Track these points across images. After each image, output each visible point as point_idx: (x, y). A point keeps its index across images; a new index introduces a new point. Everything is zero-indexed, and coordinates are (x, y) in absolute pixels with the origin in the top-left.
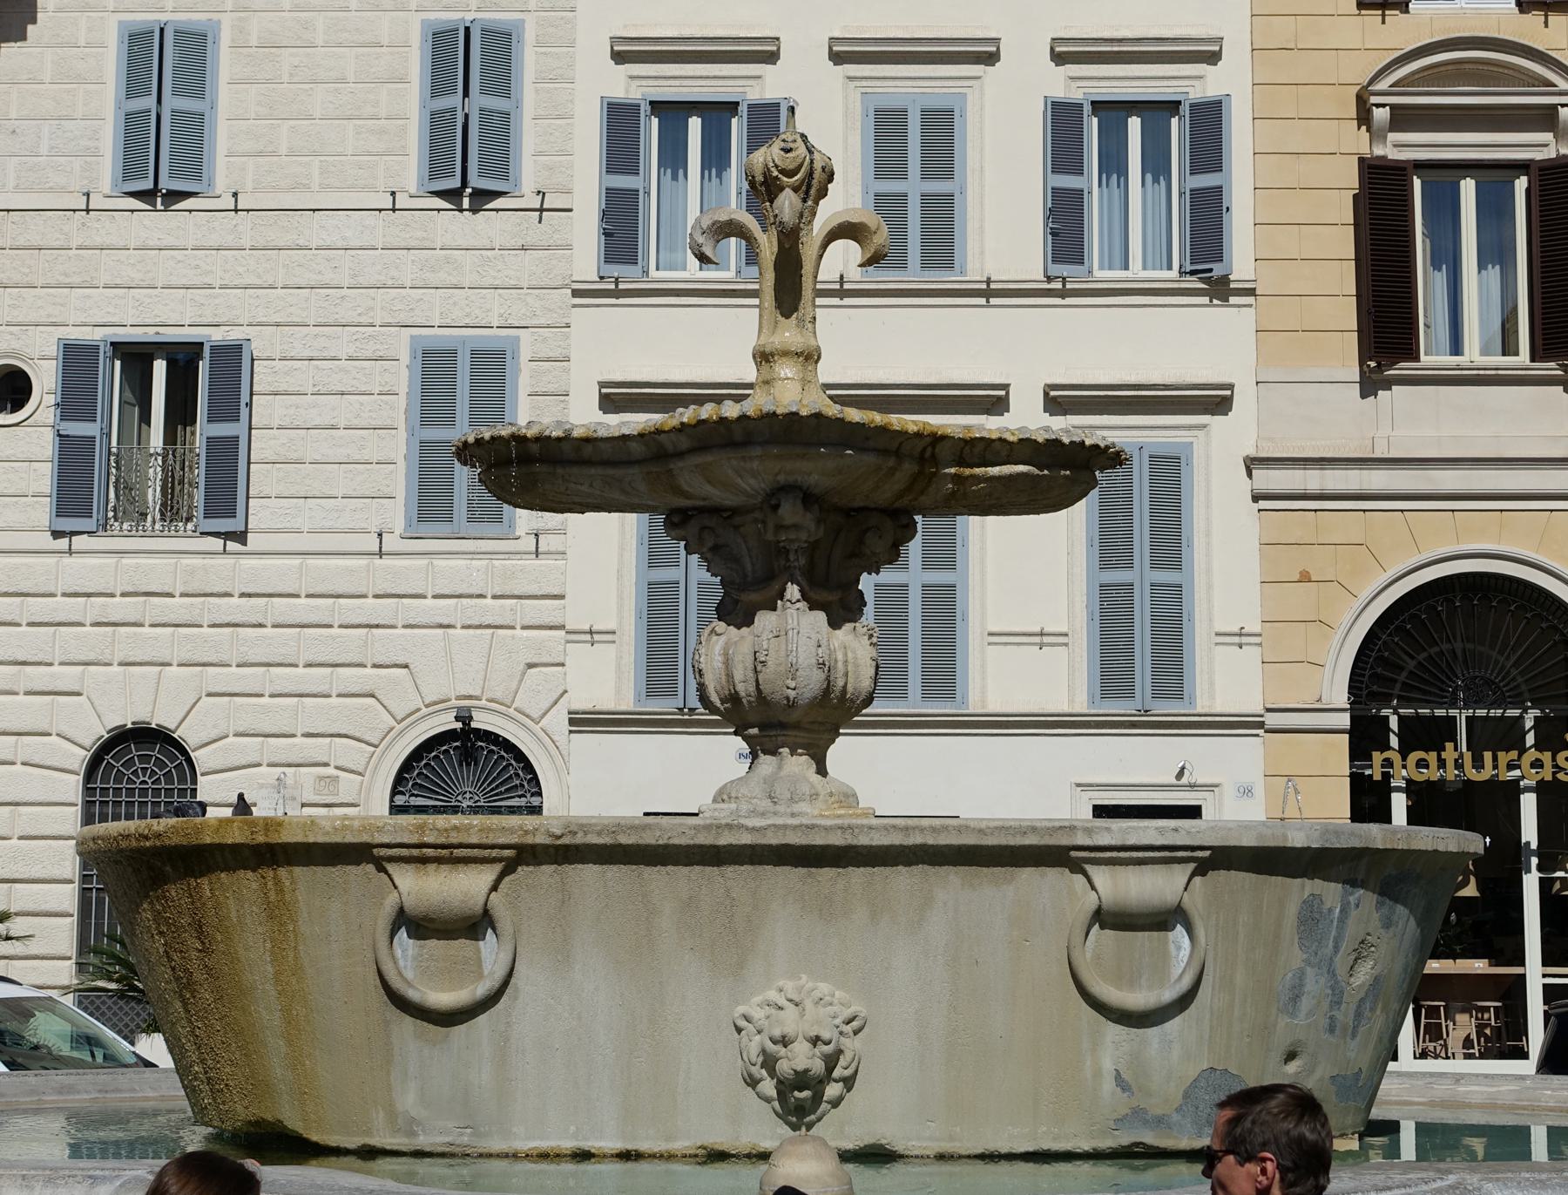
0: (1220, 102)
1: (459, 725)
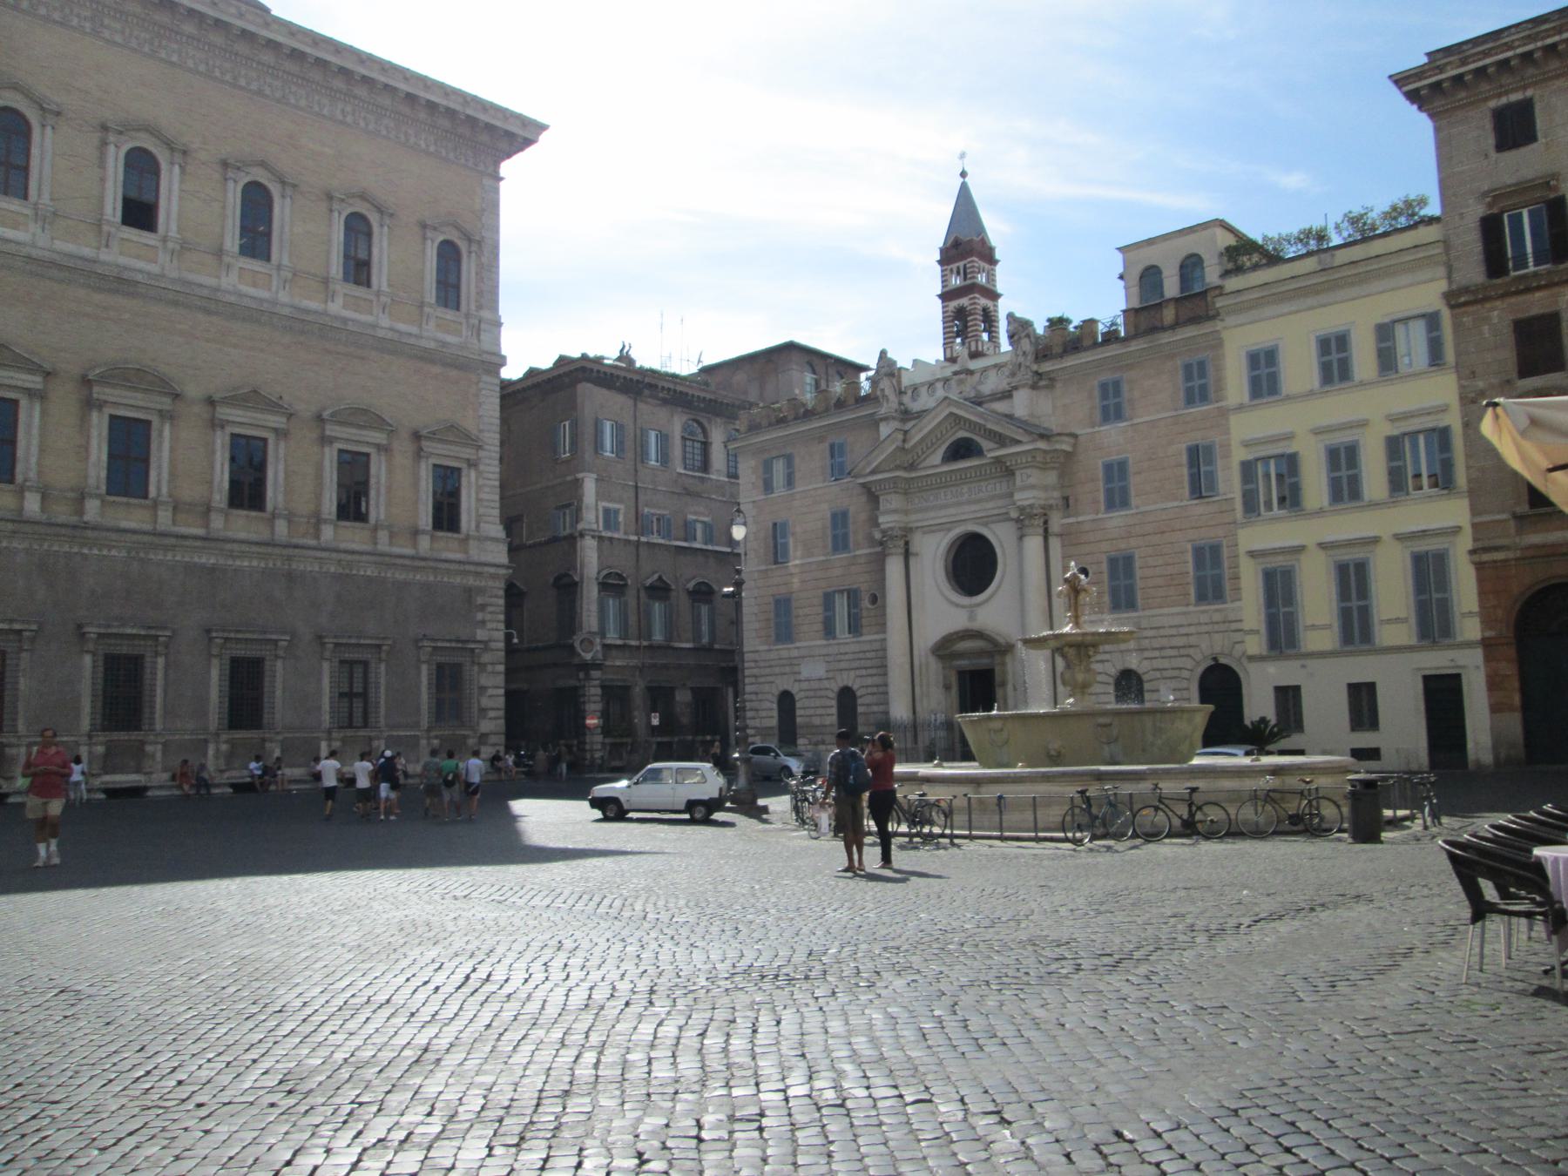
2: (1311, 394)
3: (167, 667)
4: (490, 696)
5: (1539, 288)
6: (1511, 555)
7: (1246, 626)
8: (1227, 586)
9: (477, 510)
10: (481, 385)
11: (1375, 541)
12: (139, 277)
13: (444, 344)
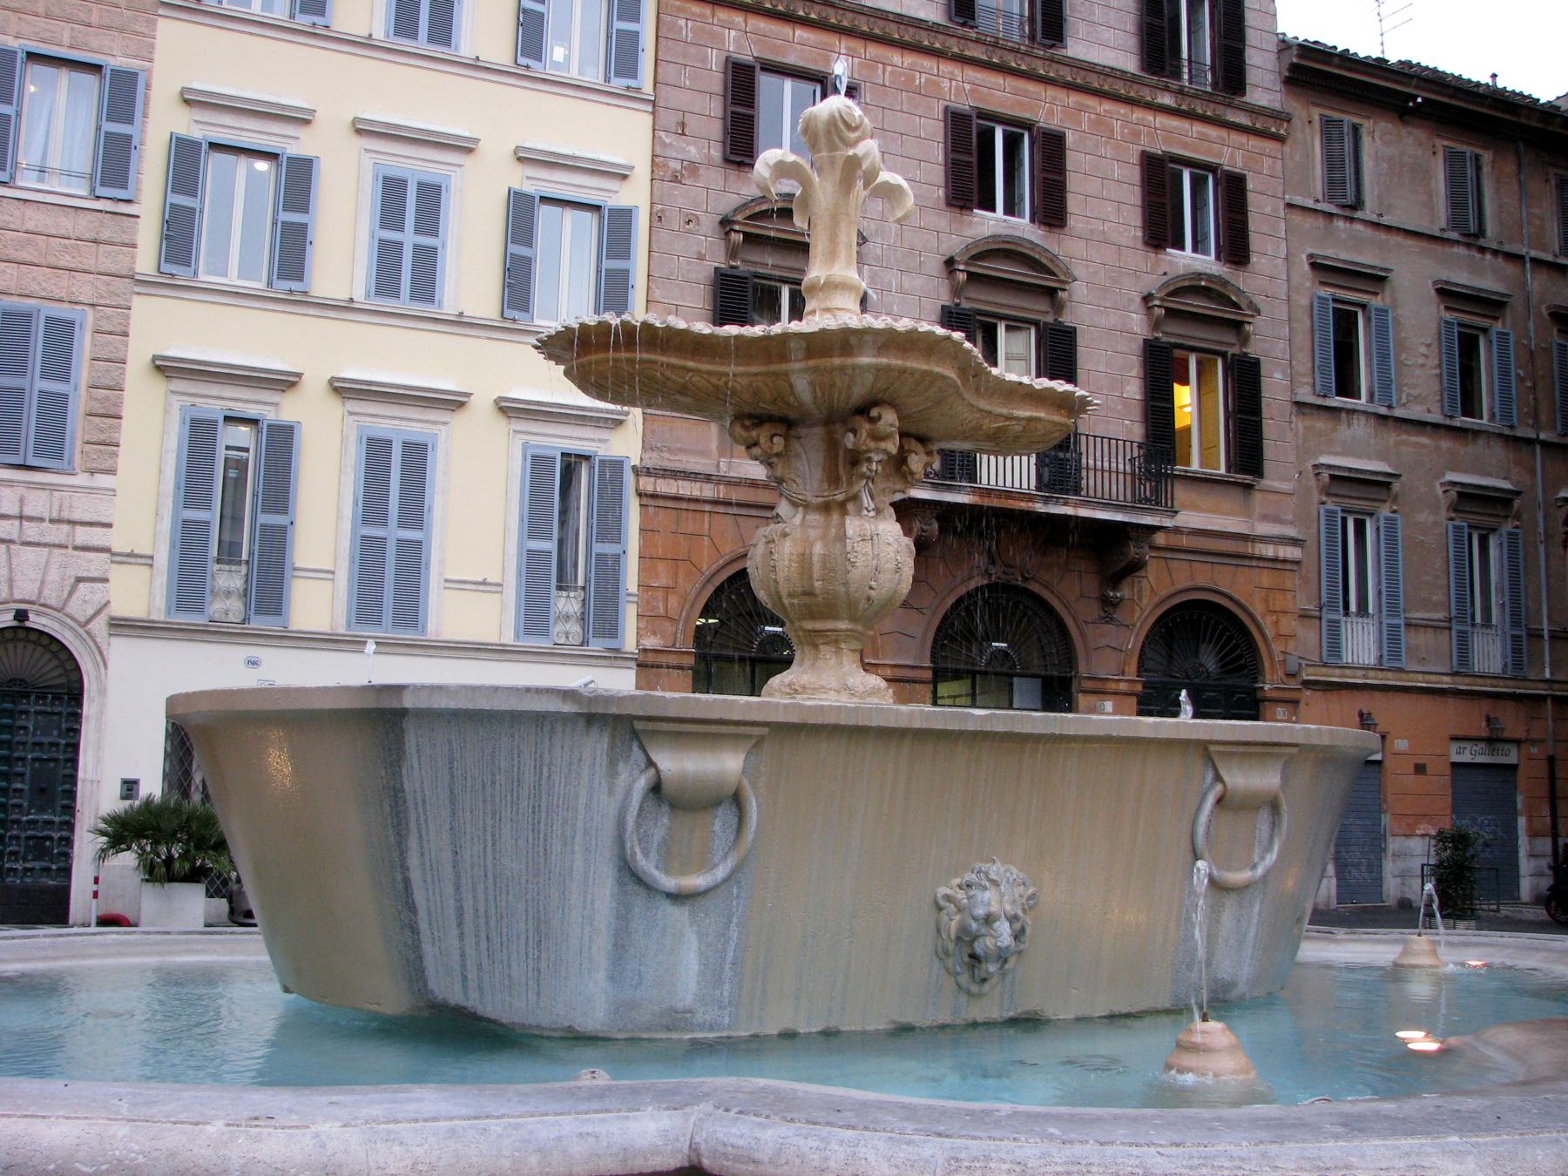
0: (631, 210)
1: (15, 623)
2: (366, 44)
5: (805, 22)
6: (708, 491)
7: (118, 540)
8: (78, 427)
11: (453, 403)
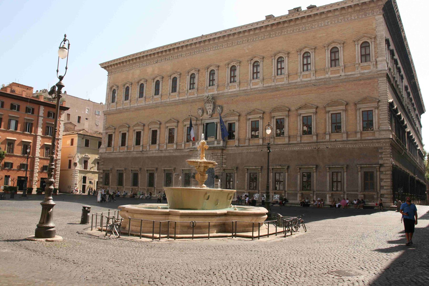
3: (288, 175)
4: (385, 182)
9: (378, 122)
10: (379, 82)
12: (279, 86)
13: (363, 74)
